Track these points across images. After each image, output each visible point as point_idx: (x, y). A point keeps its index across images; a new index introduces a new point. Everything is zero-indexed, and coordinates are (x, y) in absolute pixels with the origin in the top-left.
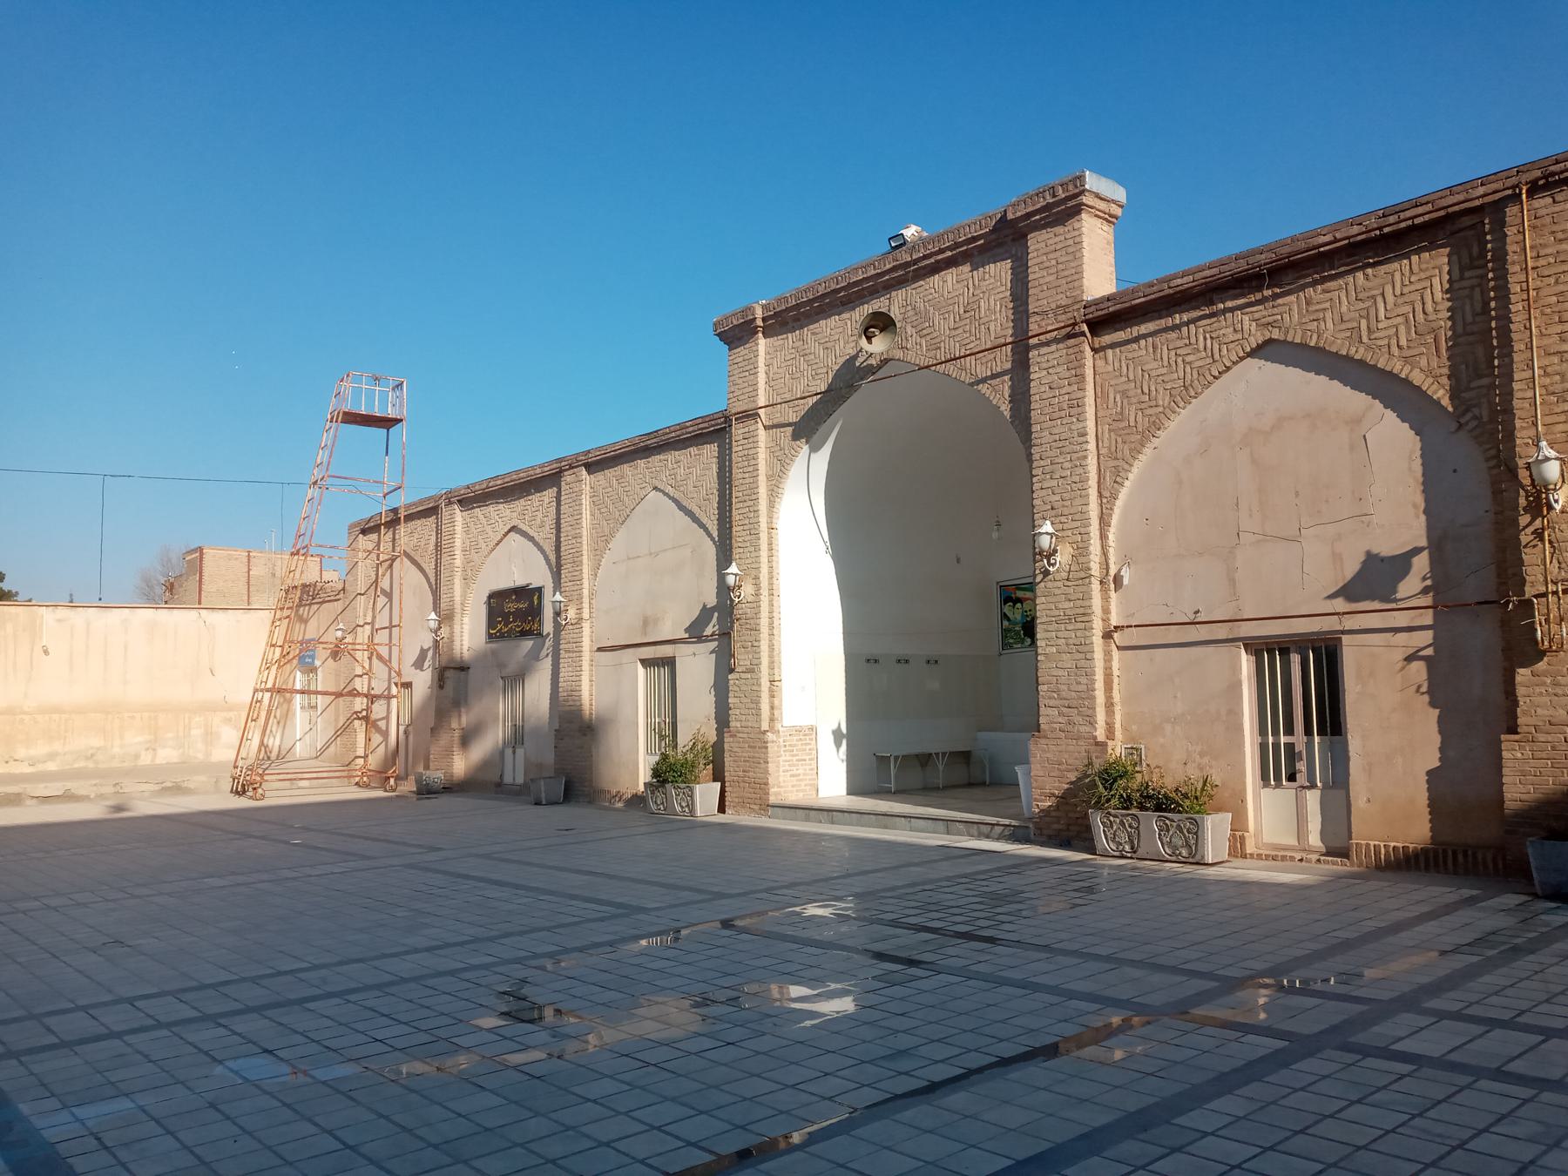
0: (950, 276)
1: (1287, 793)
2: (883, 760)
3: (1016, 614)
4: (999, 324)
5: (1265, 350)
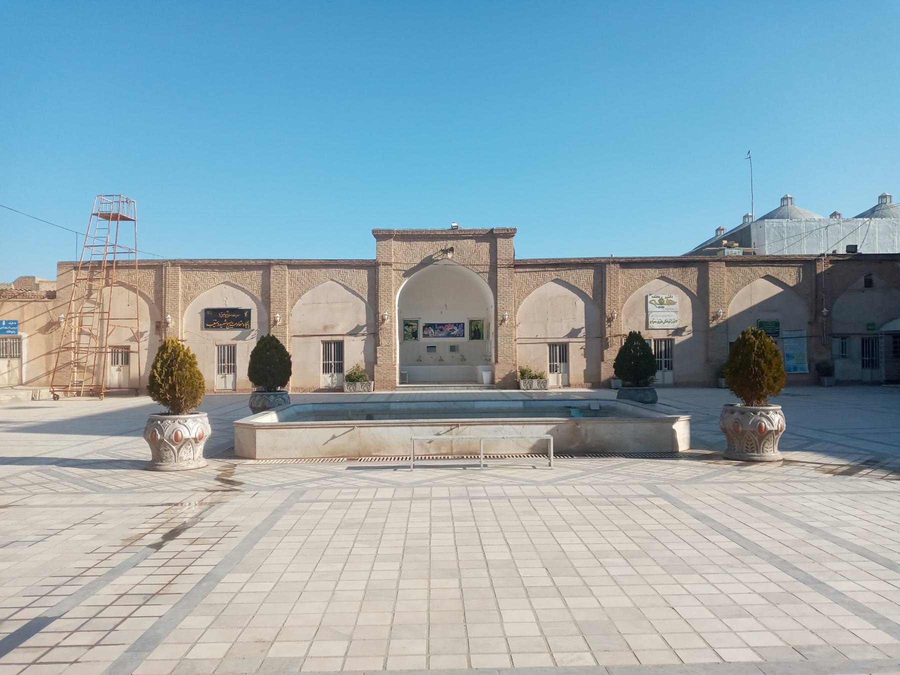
0: (470, 241)
1: (555, 374)
3: (410, 330)
4: (486, 258)
5: (557, 281)
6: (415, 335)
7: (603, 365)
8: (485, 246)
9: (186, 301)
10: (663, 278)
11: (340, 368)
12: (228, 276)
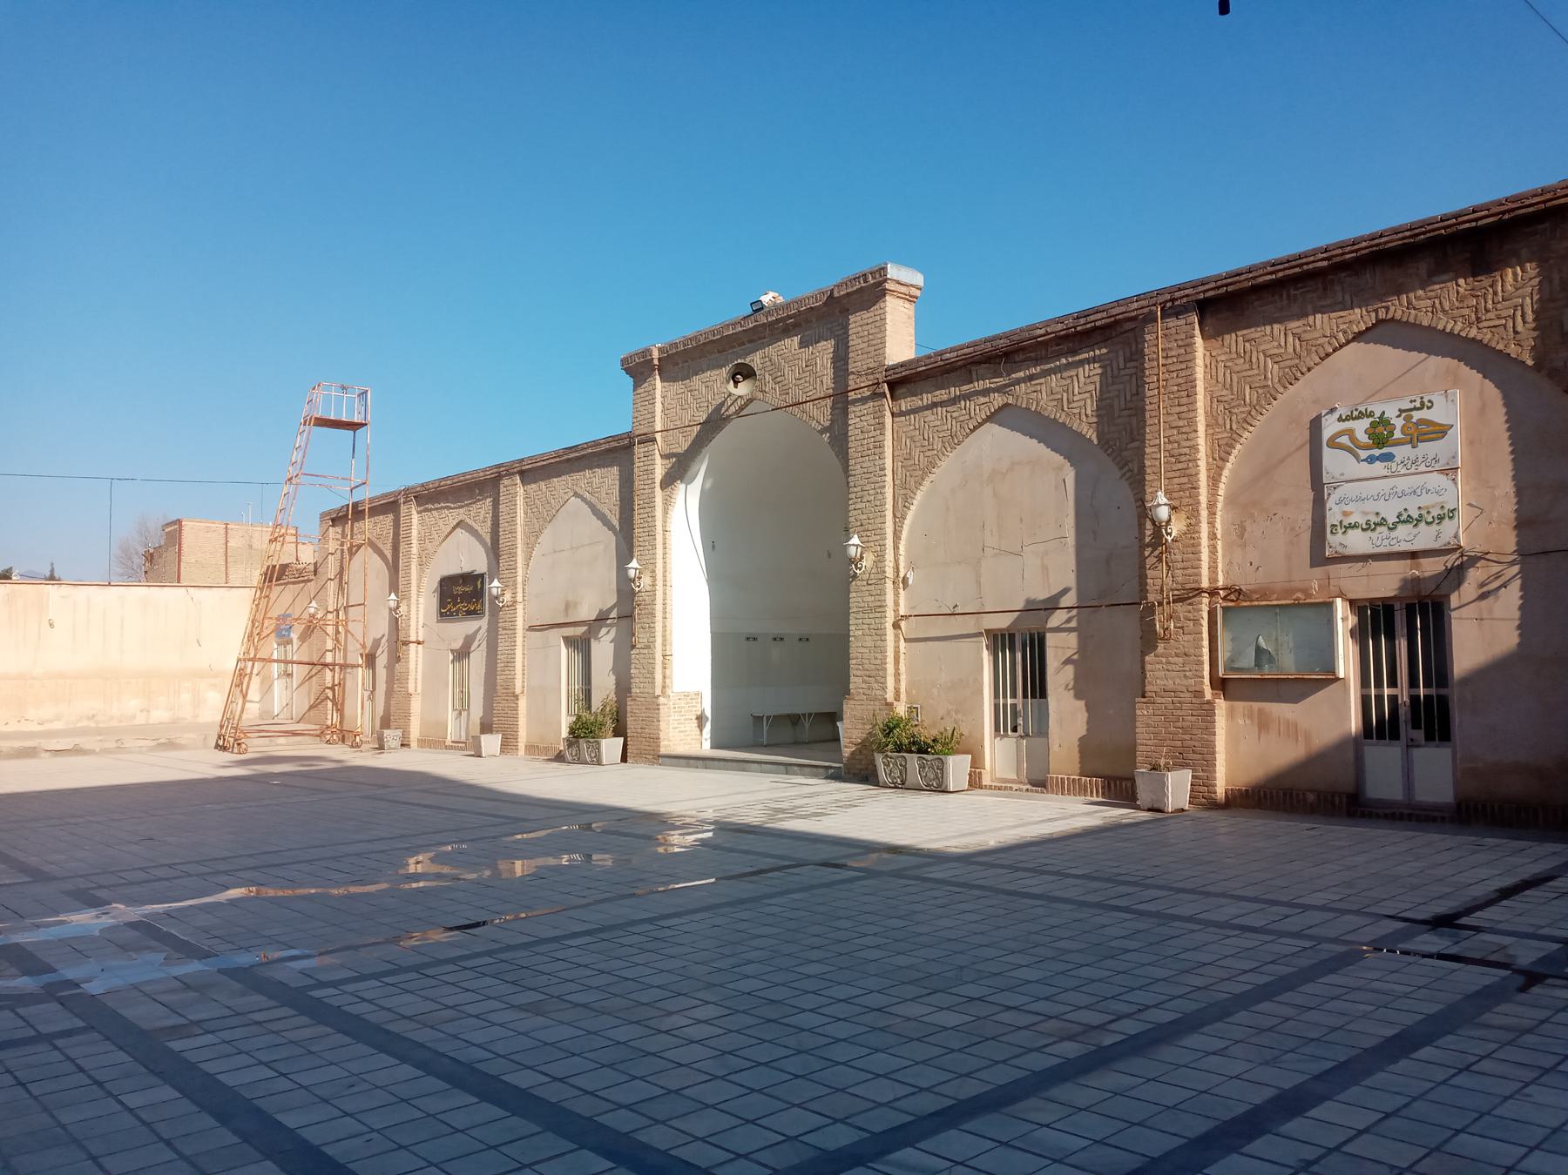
2: (758, 719)
7: (1142, 712)
10: (1381, 332)
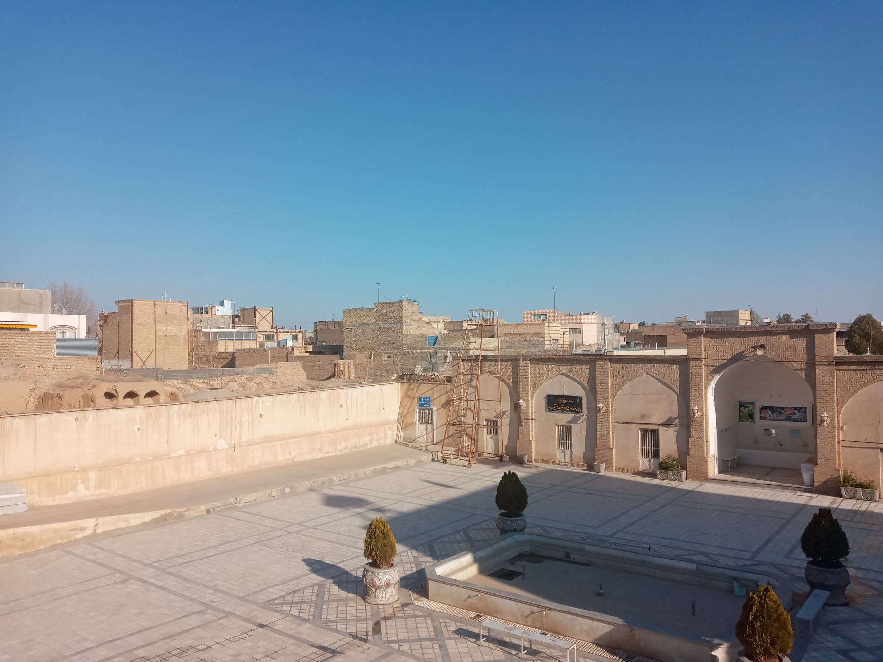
4: (803, 354)
6: (751, 416)
8: (802, 343)
9: (534, 388)
11: (656, 455)
12: (564, 369)
